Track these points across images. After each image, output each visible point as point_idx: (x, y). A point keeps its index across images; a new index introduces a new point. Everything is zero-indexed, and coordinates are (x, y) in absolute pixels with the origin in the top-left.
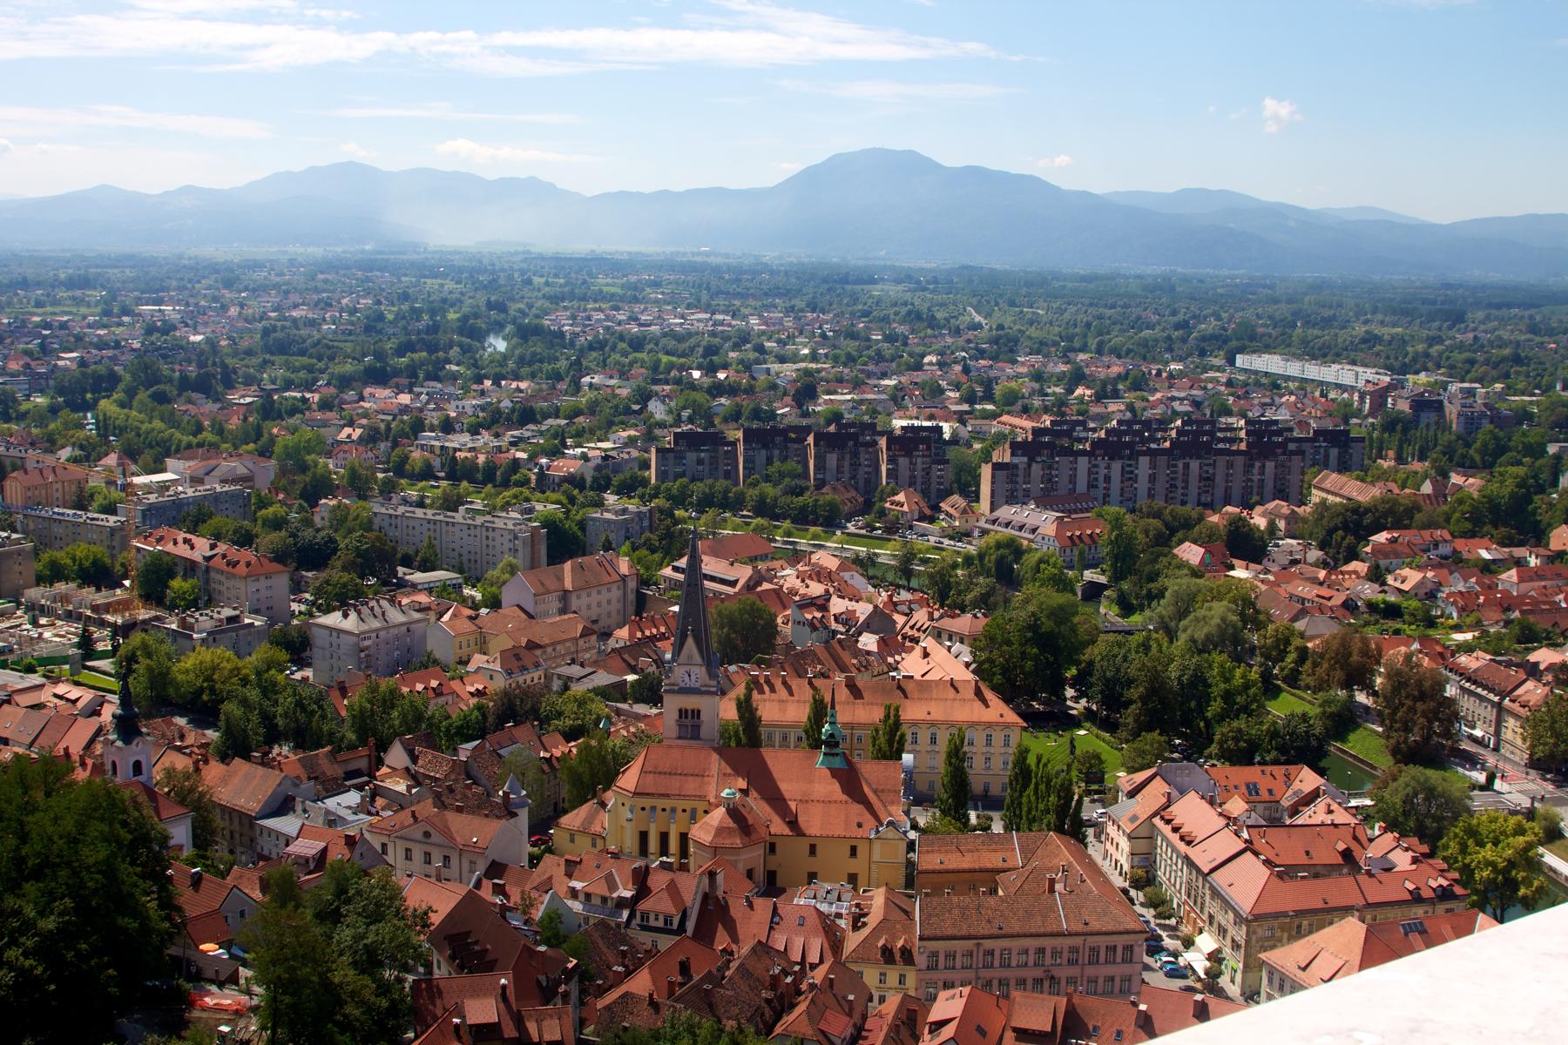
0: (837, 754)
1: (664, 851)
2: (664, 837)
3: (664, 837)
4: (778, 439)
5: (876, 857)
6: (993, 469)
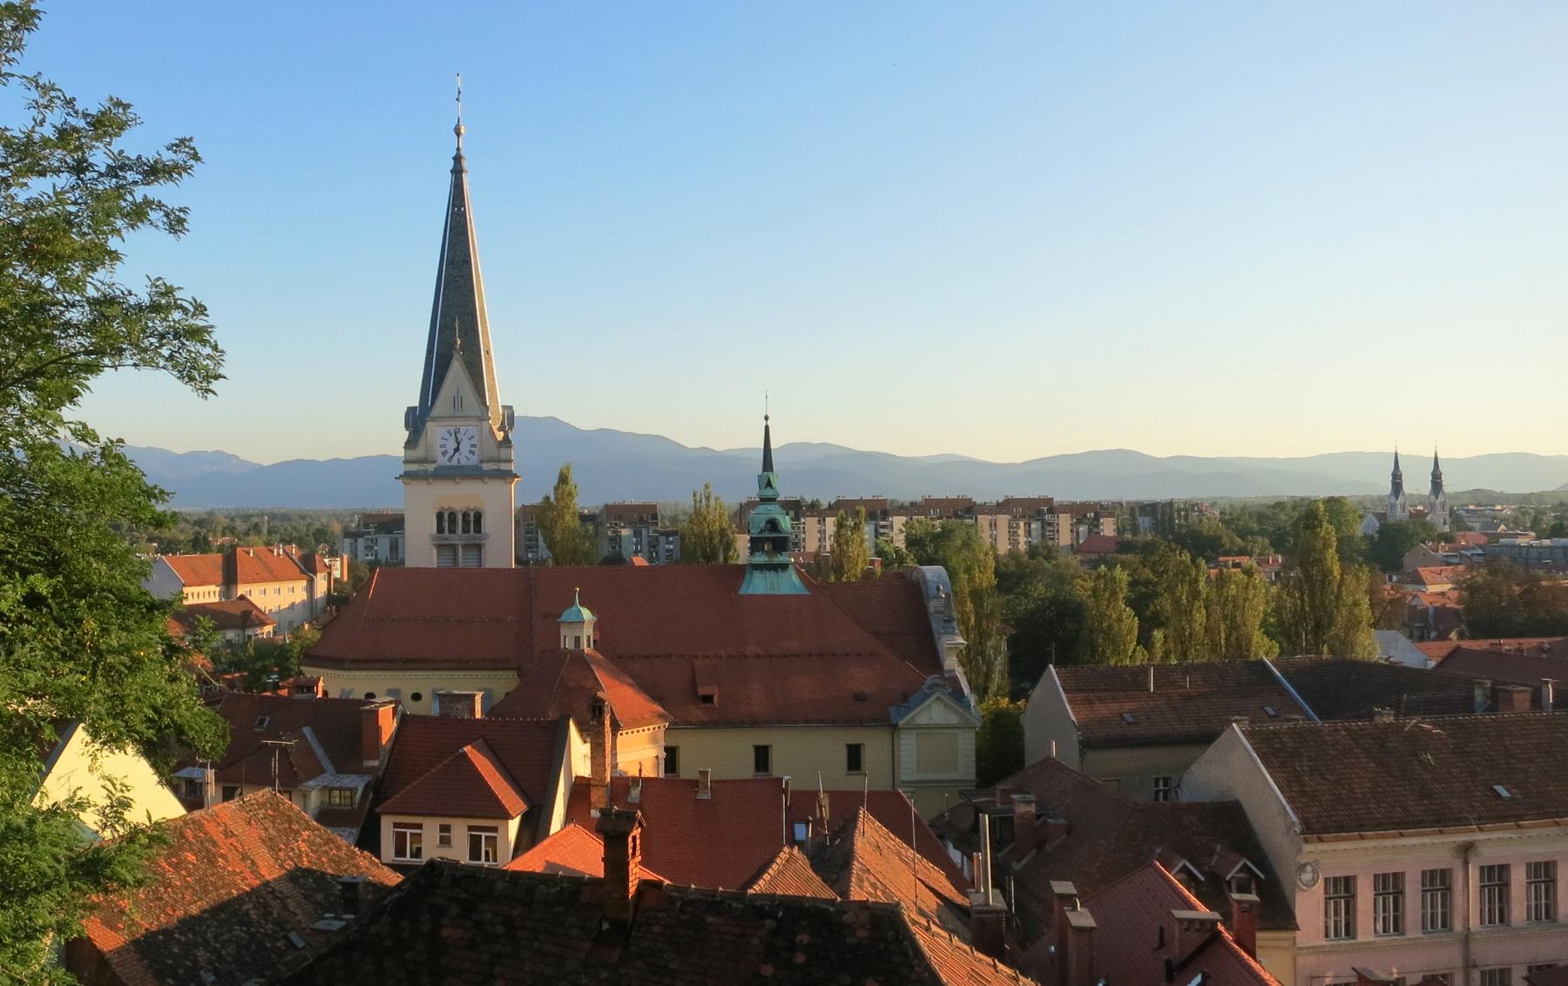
0: (784, 567)
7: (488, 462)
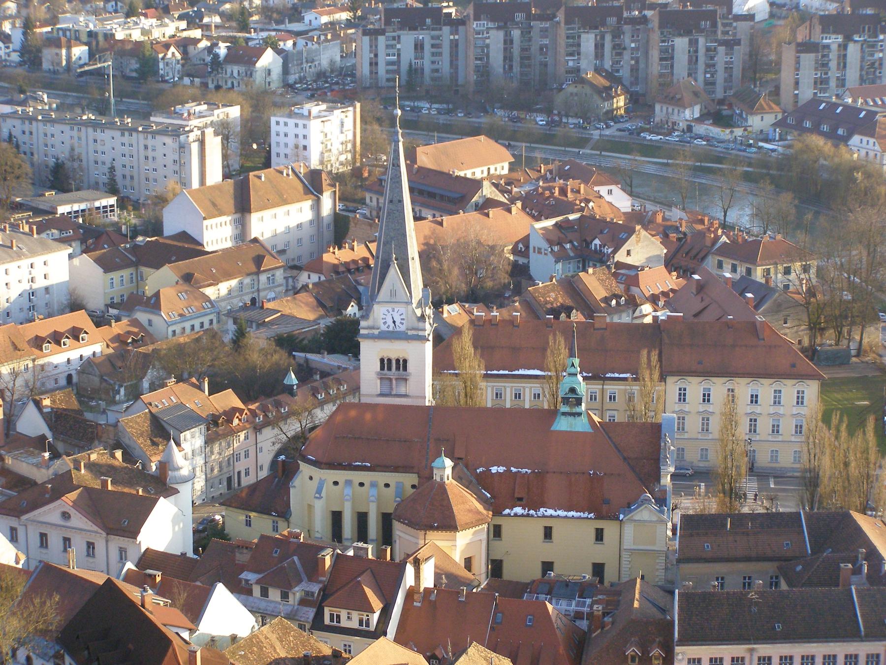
0: (579, 414)
1: (362, 535)
2: (362, 519)
3: (362, 519)
4: (519, 17)
5: (628, 543)
6: (798, 52)
7: (411, 330)
